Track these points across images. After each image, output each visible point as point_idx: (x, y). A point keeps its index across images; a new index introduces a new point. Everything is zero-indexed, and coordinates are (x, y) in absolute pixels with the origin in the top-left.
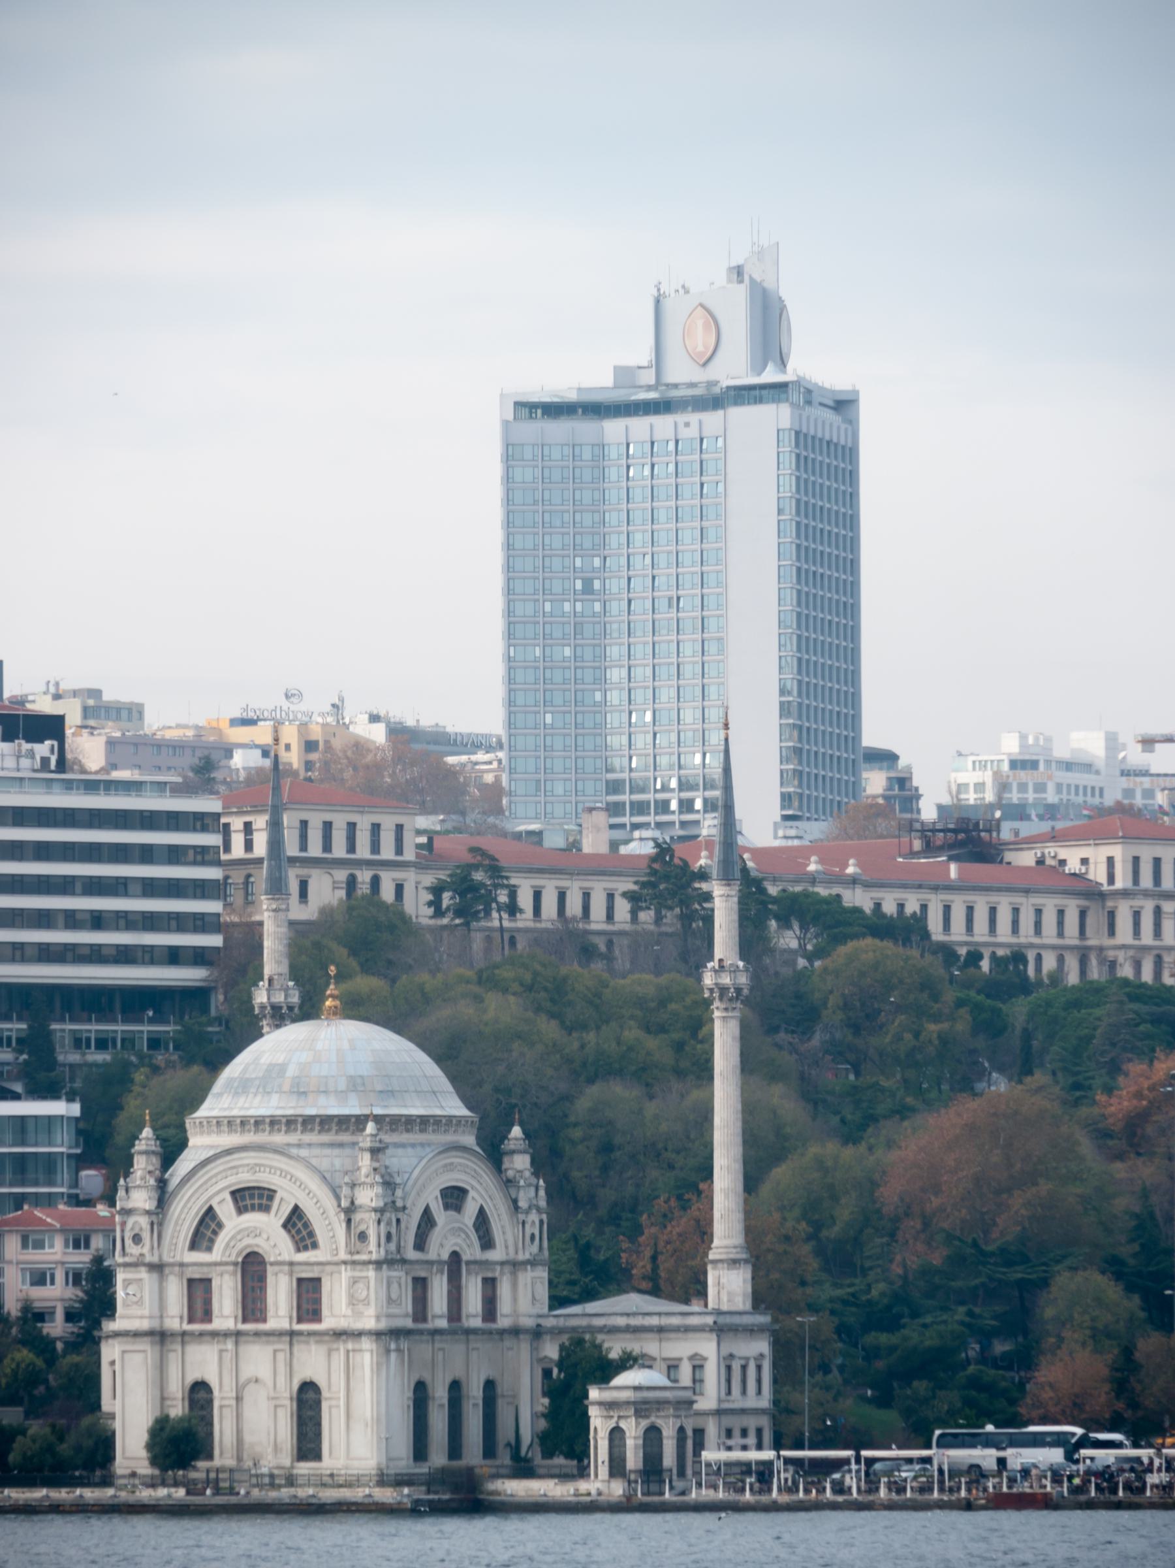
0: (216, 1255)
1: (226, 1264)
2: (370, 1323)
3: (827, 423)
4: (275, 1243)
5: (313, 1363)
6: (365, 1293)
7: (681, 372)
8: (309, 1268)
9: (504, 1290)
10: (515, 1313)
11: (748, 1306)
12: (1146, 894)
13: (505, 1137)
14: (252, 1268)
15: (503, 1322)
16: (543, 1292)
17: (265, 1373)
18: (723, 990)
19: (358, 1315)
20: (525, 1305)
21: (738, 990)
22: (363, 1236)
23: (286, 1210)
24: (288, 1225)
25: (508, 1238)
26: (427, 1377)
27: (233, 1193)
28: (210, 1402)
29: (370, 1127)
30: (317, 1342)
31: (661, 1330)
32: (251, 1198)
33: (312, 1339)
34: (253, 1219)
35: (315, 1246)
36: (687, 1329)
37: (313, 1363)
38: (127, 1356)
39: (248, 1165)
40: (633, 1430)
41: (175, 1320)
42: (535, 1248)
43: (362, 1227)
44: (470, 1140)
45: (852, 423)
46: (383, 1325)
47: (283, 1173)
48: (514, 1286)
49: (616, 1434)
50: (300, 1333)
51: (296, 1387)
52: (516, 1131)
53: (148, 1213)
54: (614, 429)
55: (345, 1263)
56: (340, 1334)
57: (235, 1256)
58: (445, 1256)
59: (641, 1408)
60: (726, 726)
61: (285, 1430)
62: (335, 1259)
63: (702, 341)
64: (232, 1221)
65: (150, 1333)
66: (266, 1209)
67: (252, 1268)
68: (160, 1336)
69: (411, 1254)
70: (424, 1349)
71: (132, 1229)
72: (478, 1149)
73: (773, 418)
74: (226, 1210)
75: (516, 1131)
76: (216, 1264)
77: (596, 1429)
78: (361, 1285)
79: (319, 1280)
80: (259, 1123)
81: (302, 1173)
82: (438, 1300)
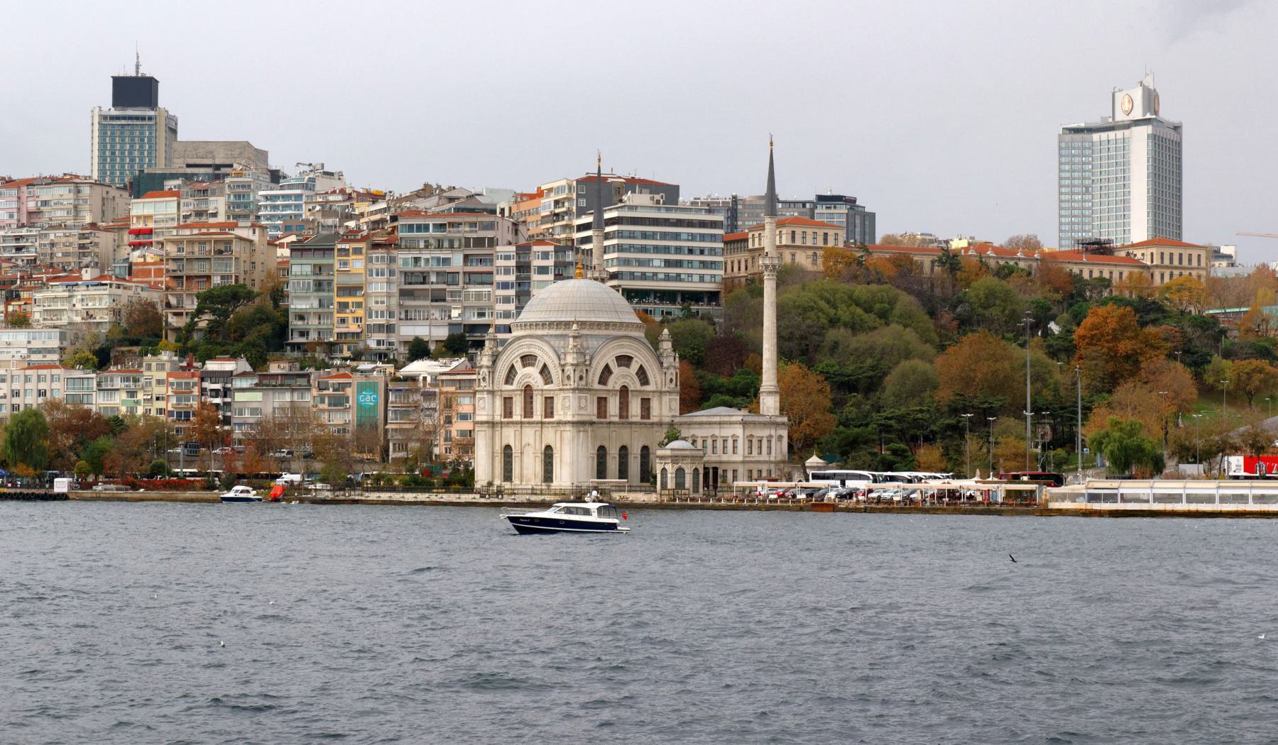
2: (569, 418)
3: (1172, 135)
4: (537, 381)
5: (550, 436)
7: (1121, 117)
9: (654, 404)
10: (661, 416)
11: (777, 413)
12: (1167, 267)
13: (660, 333)
14: (528, 391)
15: (654, 419)
16: (676, 405)
17: (532, 442)
18: (767, 266)
19: (565, 414)
20: (665, 412)
21: (774, 266)
22: (568, 377)
23: (541, 366)
24: (541, 372)
25: (656, 379)
26: (606, 444)
27: (522, 358)
29: (575, 327)
31: (720, 423)
32: (528, 360)
34: (529, 370)
36: (731, 423)
37: (550, 436)
40: (671, 469)
42: (673, 385)
44: (640, 334)
45: (1180, 134)
46: (576, 419)
47: (540, 349)
48: (661, 402)
52: (666, 331)
54: (1096, 137)
56: (559, 423)
58: (618, 388)
59: (675, 459)
61: (539, 469)
63: (1127, 106)
64: (521, 371)
65: (487, 422)
66: (533, 365)
68: (492, 424)
69: (596, 386)
70: (604, 431)
72: (646, 341)
73: (1146, 130)
74: (518, 365)
75: (666, 331)
82: (613, 406)
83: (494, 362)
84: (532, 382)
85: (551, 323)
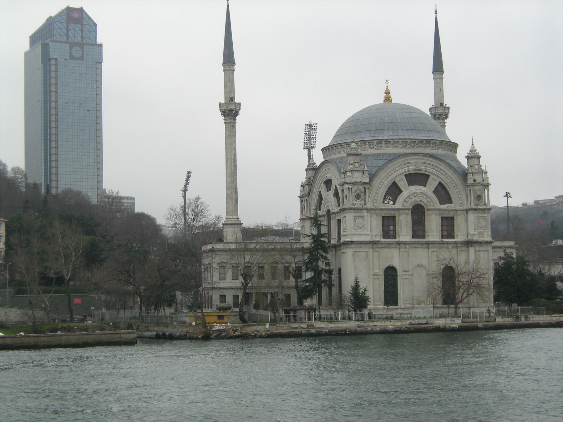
1: (406, 209)
6: (484, 224)
8: (447, 212)
14: (418, 213)
19: (481, 234)
22: (479, 197)
23: (435, 184)
24: (436, 192)
28: (396, 276)
30: (453, 247)
33: (450, 246)
38: (356, 254)
39: (415, 163)
53: (365, 184)
57: (409, 205)
60: (436, 12)
62: (462, 208)
67: (418, 213)
71: (356, 192)
74: (402, 183)
76: (398, 210)
79: (452, 218)
81: (443, 167)
83: (371, 180)
84: (423, 201)
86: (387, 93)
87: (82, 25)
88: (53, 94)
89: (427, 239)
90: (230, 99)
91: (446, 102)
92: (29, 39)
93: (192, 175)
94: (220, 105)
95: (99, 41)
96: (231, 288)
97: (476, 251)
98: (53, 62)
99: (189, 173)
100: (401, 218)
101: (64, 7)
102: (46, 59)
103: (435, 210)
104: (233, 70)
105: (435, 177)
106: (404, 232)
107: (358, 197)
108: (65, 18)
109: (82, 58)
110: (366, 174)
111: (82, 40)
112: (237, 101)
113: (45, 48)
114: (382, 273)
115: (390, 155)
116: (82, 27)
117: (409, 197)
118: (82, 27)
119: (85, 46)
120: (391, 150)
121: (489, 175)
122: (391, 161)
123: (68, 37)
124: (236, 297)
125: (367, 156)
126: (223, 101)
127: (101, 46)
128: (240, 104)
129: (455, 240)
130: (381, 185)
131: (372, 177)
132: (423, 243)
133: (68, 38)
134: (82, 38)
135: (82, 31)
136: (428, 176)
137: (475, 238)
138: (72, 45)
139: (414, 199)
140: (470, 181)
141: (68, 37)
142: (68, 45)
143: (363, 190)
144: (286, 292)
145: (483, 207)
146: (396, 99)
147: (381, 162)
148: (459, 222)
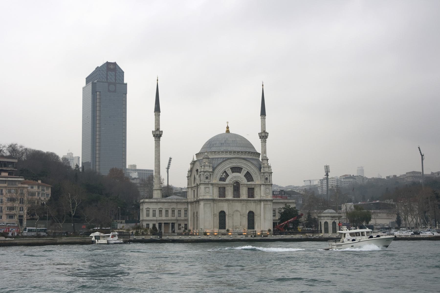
0: (227, 181)
5: (252, 207)
17: (239, 209)
22: (267, 179)
23: (245, 172)
33: (252, 202)
35: (252, 180)
37: (252, 207)
41: (216, 197)
43: (267, 177)
49: (334, 223)
50: (250, 200)
51: (248, 212)
53: (210, 172)
55: (263, 184)
56: (260, 201)
61: (245, 222)
68: (214, 200)
74: (229, 172)
76: (227, 184)
77: (326, 223)
78: (267, 189)
80: (238, 152)
81: (249, 164)
85: (249, 152)
86: (228, 128)
87: (116, 73)
88: (98, 112)
89: (240, 198)
90: (158, 129)
91: (267, 131)
92: (85, 80)
93: (172, 160)
94: (153, 131)
95: (125, 82)
96: (152, 220)
97: (264, 204)
98: (98, 93)
99: (170, 159)
100: (228, 188)
101: (105, 62)
102: (94, 92)
103: (245, 184)
104: (159, 115)
105: (245, 169)
106: (229, 195)
107: (207, 178)
108: (106, 68)
109: (115, 91)
110: (211, 167)
111: (115, 81)
112: (161, 130)
113: (94, 85)
114: (218, 214)
115: (224, 158)
116: (115, 74)
117: (232, 178)
118: (115, 74)
119: (117, 85)
120: (224, 156)
121: (272, 168)
122: (224, 161)
123: (107, 79)
124: (154, 225)
125: (213, 159)
126: (154, 130)
127: (126, 84)
128: (162, 131)
129: (255, 199)
130: (219, 173)
131: (214, 169)
132: (238, 200)
133: (107, 80)
134: (115, 80)
135: (116, 76)
136: (242, 168)
137: (264, 198)
138: (110, 84)
139: (235, 179)
140: (262, 171)
141: (107, 79)
142: (107, 84)
143: (209, 175)
144: (179, 222)
145: (269, 183)
146: (231, 131)
147: (219, 162)
148: (257, 190)
